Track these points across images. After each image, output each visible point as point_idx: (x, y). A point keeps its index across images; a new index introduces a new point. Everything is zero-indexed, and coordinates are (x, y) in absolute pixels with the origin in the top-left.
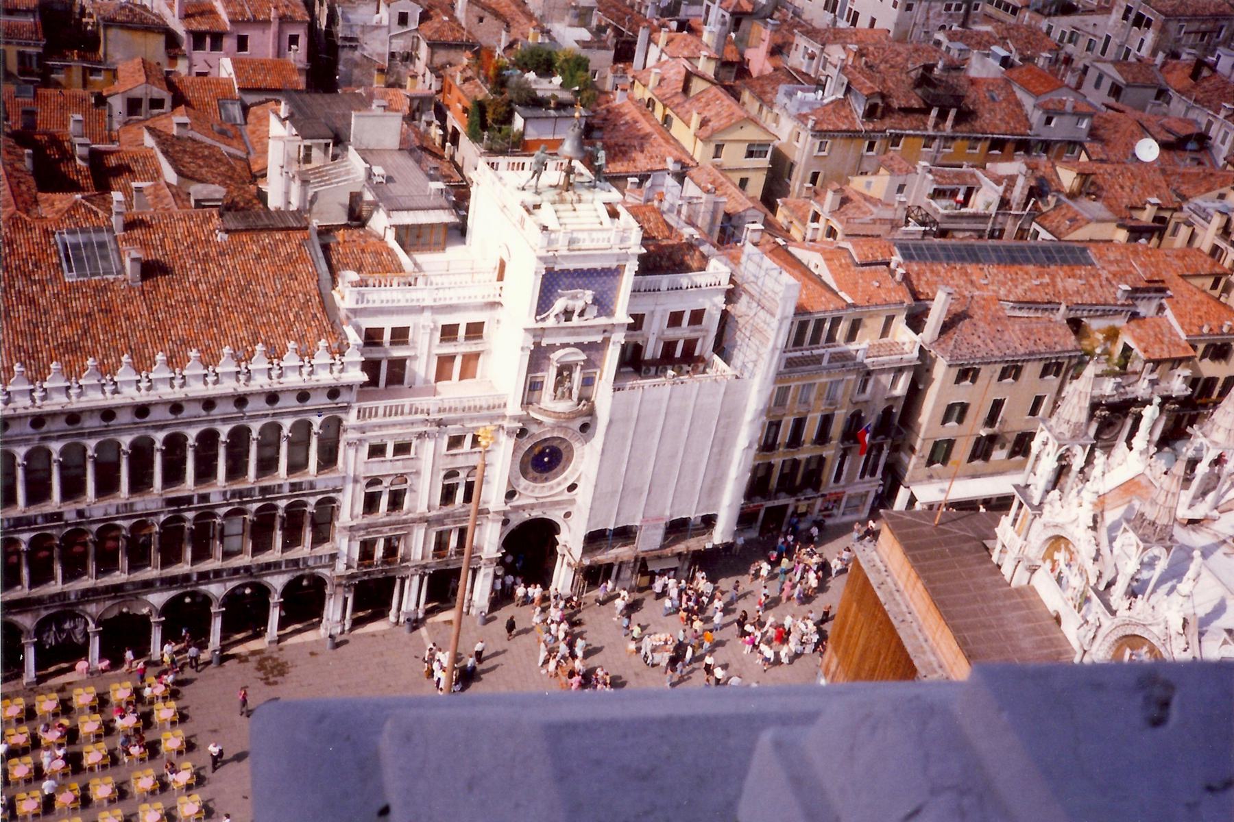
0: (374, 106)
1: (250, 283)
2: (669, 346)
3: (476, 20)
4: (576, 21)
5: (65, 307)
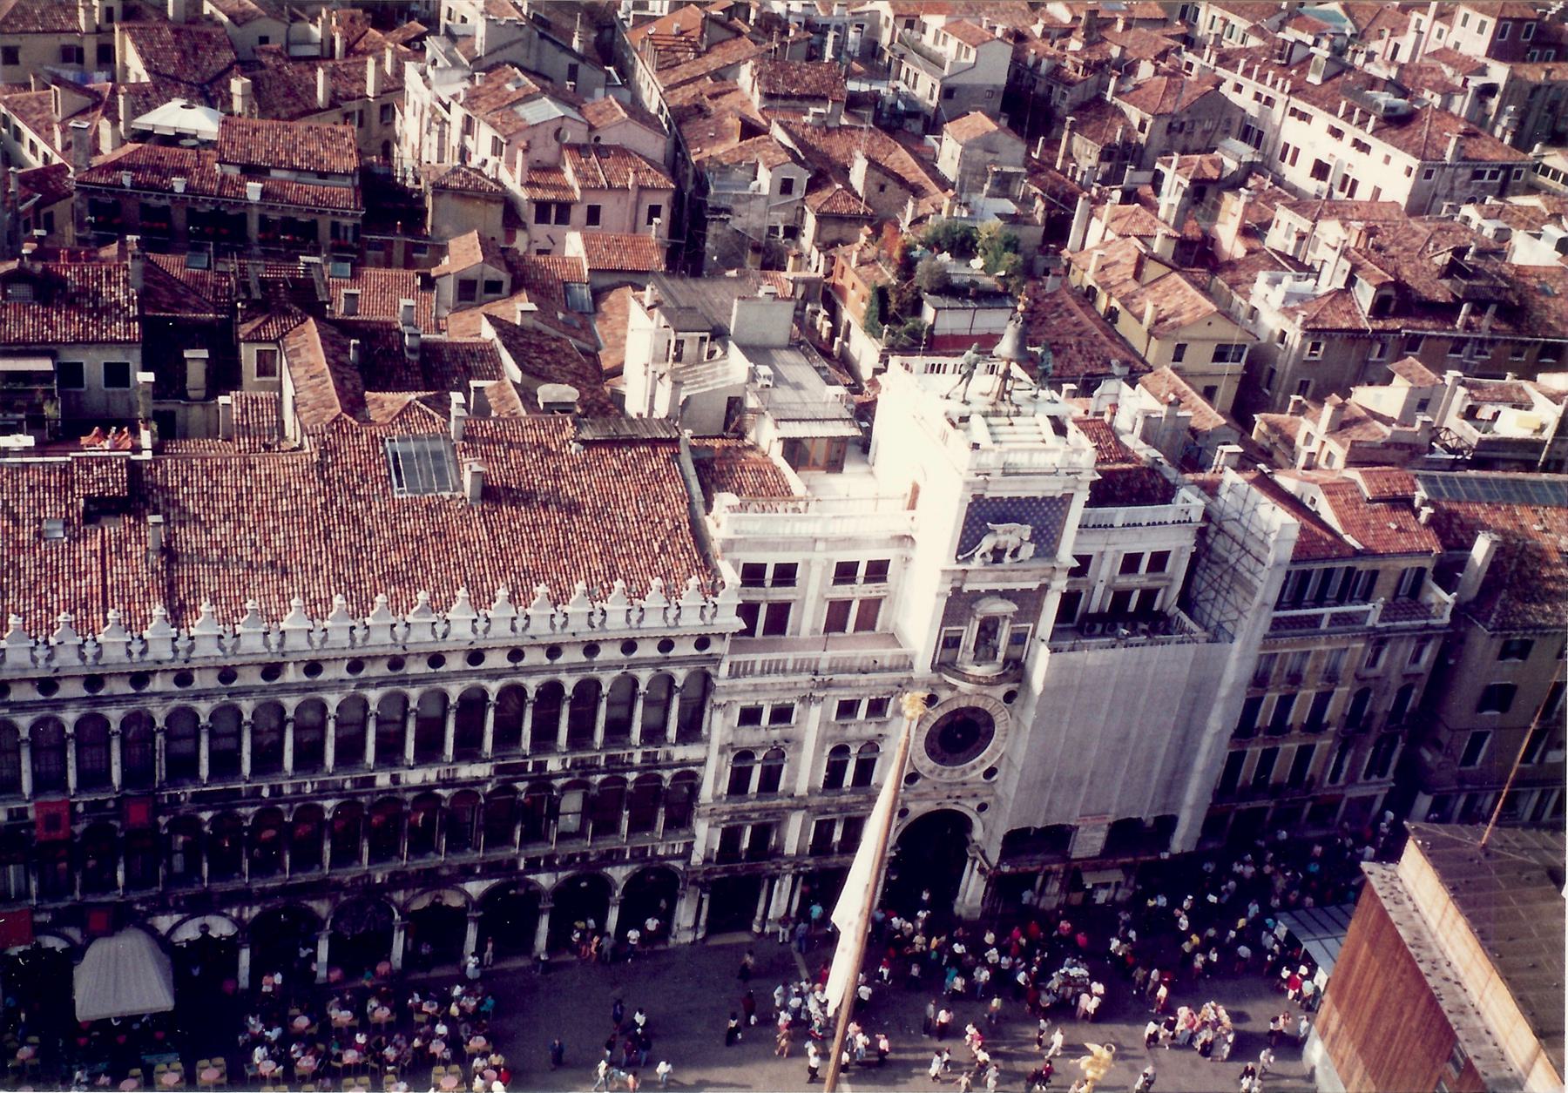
0: (761, 294)
1: (607, 504)
2: (1121, 597)
3: (875, 189)
4: (997, 191)
5: (394, 527)
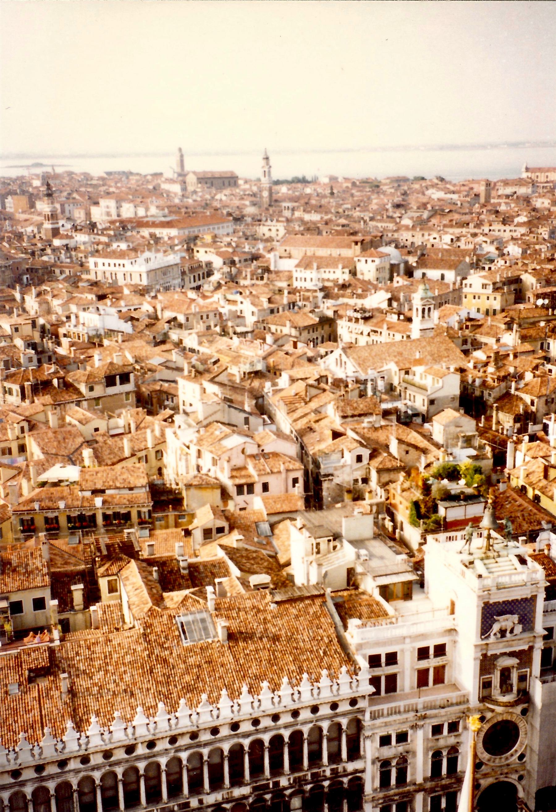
0: (356, 513)
1: (293, 634)
3: (404, 453)
4: (465, 445)
5: (185, 662)
